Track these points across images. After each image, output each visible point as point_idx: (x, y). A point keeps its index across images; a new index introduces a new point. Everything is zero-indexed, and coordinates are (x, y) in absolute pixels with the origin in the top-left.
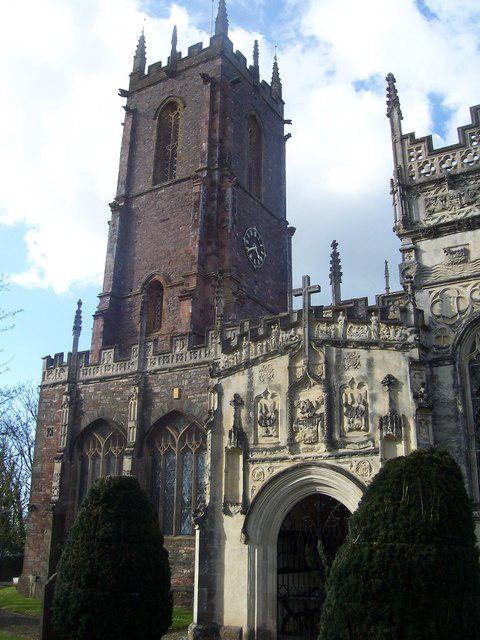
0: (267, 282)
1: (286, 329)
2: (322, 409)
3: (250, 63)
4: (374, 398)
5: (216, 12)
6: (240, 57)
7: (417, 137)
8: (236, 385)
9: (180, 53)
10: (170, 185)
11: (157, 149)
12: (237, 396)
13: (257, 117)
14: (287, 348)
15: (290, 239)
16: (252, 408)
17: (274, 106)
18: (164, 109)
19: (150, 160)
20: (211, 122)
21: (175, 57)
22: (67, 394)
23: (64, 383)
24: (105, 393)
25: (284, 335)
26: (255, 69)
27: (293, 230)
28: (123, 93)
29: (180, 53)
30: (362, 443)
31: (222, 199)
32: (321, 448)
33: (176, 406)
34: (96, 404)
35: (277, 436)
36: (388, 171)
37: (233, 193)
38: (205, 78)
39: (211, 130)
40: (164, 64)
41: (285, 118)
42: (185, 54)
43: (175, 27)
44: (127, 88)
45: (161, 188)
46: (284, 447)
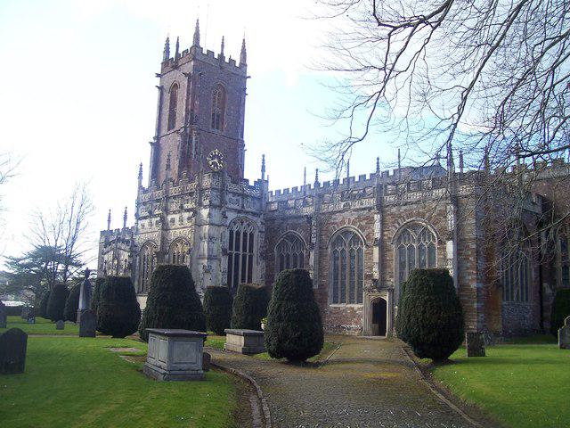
19: (167, 117)
20: (187, 100)
26: (222, 56)
28: (158, 75)
31: (190, 143)
37: (196, 139)
39: (187, 105)
41: (248, 75)
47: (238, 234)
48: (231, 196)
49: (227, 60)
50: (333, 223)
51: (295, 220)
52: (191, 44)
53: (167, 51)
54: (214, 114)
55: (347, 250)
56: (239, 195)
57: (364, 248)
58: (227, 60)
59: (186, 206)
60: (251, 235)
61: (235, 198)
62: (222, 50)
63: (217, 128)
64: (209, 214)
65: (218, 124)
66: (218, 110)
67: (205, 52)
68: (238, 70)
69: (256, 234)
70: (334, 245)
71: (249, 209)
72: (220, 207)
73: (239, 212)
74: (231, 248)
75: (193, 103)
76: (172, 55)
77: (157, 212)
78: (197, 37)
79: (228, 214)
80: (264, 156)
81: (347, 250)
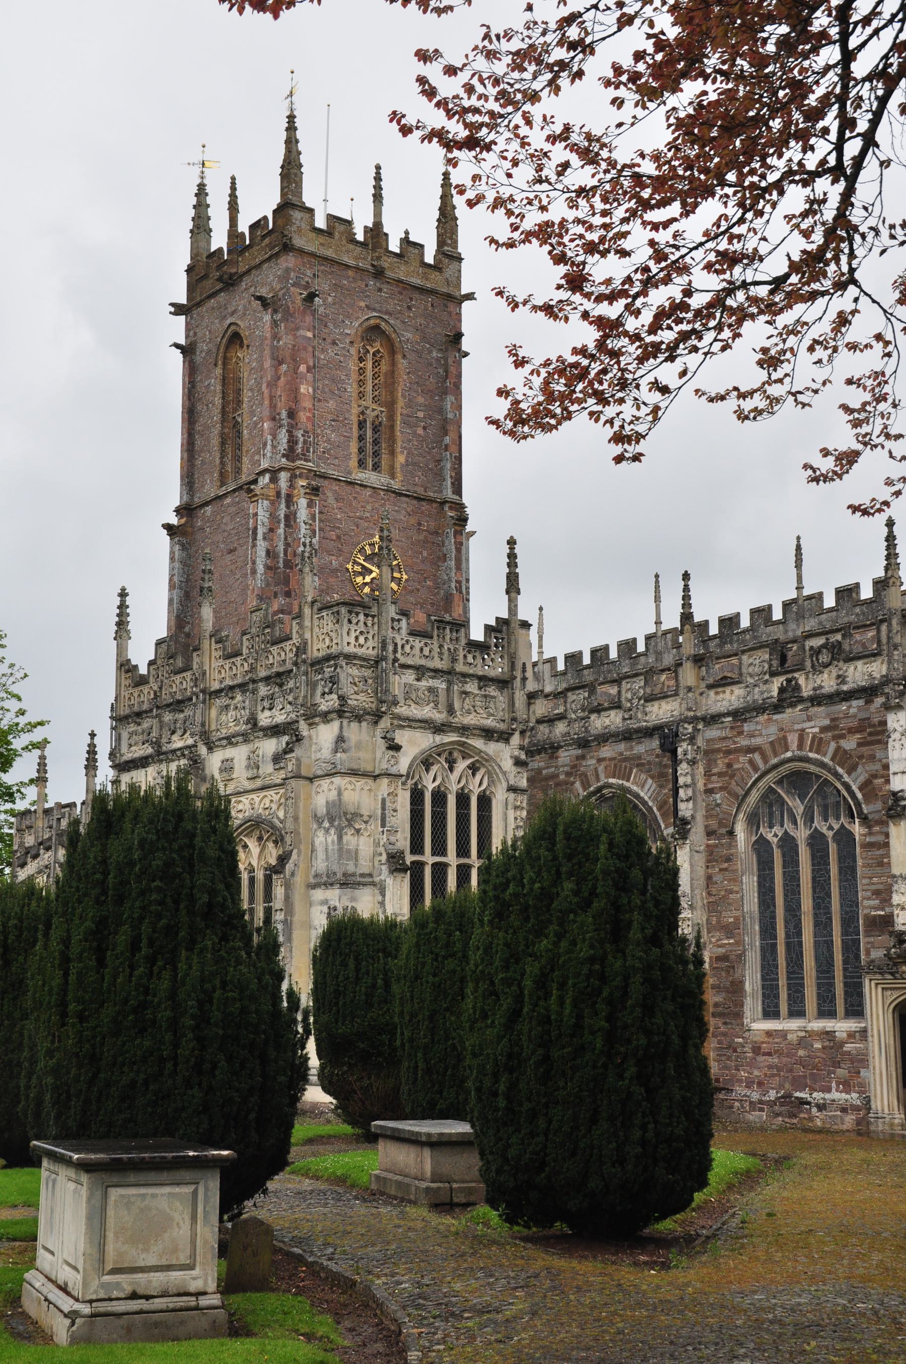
11: (223, 422)
18: (227, 347)
26: (376, 232)
28: (179, 310)
31: (290, 518)
37: (310, 505)
43: (233, 179)
44: (183, 300)
47: (439, 798)
48: (409, 677)
49: (394, 246)
50: (750, 750)
51: (622, 746)
52: (274, 199)
54: (361, 425)
55: (801, 834)
56: (436, 673)
57: (857, 829)
58: (394, 246)
59: (265, 719)
60: (485, 802)
61: (424, 683)
62: (378, 213)
63: (376, 467)
64: (340, 739)
65: (376, 454)
66: (374, 411)
67: (320, 222)
68: (435, 275)
69: (500, 797)
70: (753, 821)
71: (470, 720)
72: (377, 716)
73: (439, 729)
74: (417, 846)
76: (219, 240)
77: (178, 743)
78: (291, 171)
79: (402, 737)
80: (512, 542)
81: (801, 834)
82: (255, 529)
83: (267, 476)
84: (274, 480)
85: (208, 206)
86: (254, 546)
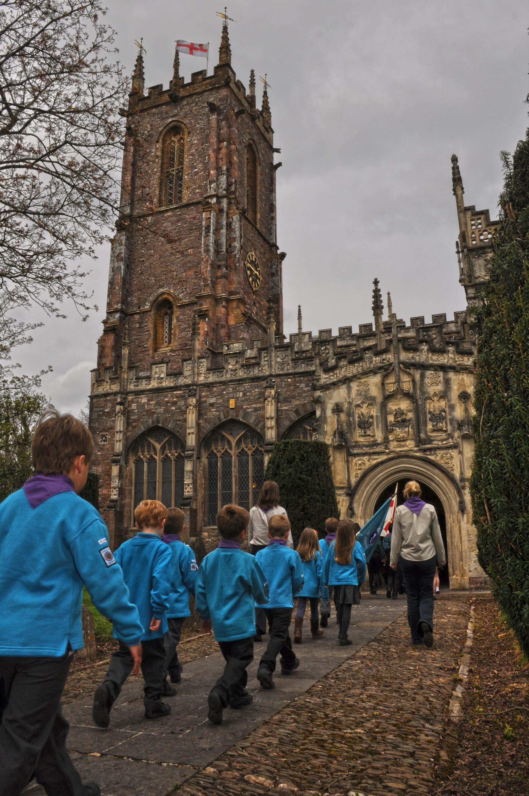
0: (262, 303)
1: (377, 354)
2: (410, 415)
3: (248, 92)
4: (452, 407)
5: (220, 41)
6: (239, 86)
7: (478, 209)
8: (339, 395)
9: (183, 78)
10: (176, 208)
11: (162, 172)
12: (337, 405)
13: (254, 145)
14: (380, 368)
15: (281, 263)
16: (349, 414)
17: (266, 134)
18: (167, 133)
21: (177, 81)
22: (121, 404)
23: (115, 394)
24: (158, 404)
25: (377, 360)
26: (252, 100)
27: (283, 255)
29: (183, 78)
30: (445, 440)
31: (229, 225)
32: (410, 444)
33: (232, 415)
34: (150, 413)
35: (374, 436)
36: (455, 237)
38: (213, 108)
40: (166, 87)
41: (275, 146)
42: (188, 80)
45: (167, 211)
46: (379, 444)
53: (139, 74)
75: (229, 155)
78: (225, 49)
82: (208, 228)
83: (215, 200)
84: (219, 202)
85: (143, 67)
86: (207, 236)
